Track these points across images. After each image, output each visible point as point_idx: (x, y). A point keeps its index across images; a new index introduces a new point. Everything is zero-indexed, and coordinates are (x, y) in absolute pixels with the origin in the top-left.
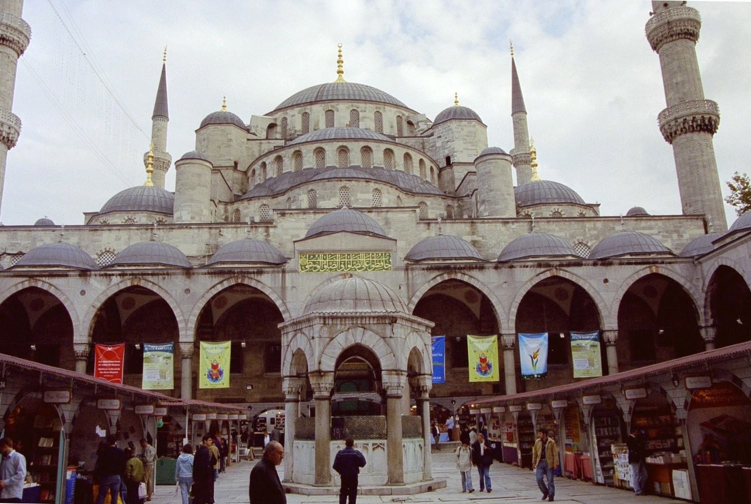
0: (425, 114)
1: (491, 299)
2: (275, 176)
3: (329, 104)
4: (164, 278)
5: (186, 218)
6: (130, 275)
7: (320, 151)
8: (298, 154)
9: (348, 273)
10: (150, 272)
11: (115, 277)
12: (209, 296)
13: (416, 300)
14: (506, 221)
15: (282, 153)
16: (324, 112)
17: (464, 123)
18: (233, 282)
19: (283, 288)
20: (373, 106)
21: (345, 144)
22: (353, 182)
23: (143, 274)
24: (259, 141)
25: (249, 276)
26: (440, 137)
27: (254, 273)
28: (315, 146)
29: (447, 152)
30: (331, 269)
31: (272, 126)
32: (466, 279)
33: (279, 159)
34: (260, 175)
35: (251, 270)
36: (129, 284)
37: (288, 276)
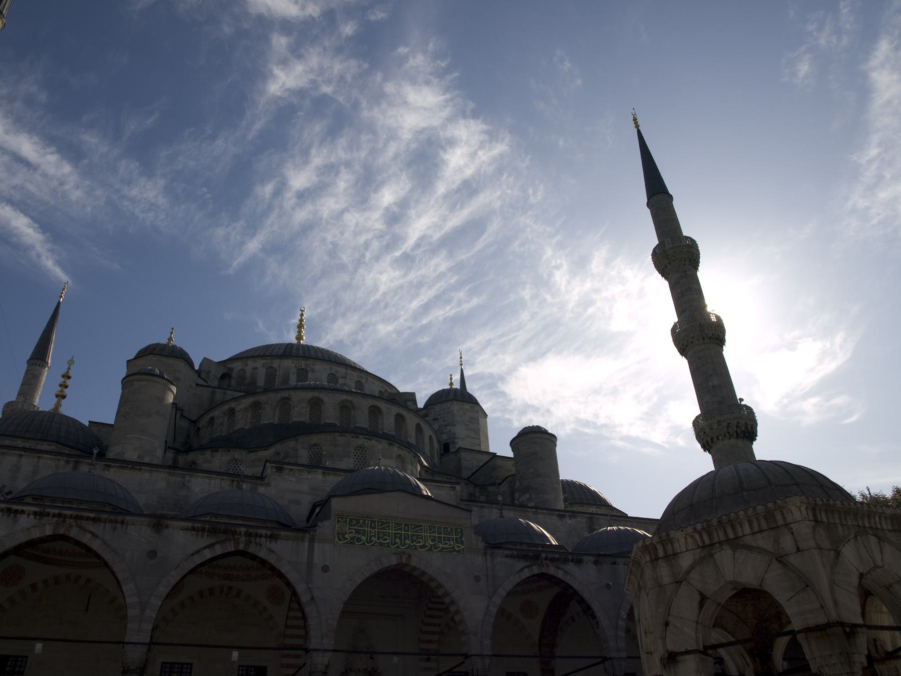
0: (413, 394)
1: (593, 606)
2: (247, 428)
3: (303, 362)
4: (115, 529)
5: (131, 455)
6: (54, 516)
7: (316, 404)
8: (286, 401)
9: (404, 552)
10: (92, 515)
11: (25, 516)
12: (190, 565)
13: (497, 600)
14: (561, 515)
15: (262, 398)
16: (295, 370)
17: (467, 406)
18: (231, 548)
19: (310, 565)
20: (356, 374)
21: (350, 398)
22: (373, 442)
23: (77, 518)
24: (210, 389)
25: (258, 540)
26: (437, 419)
27: (266, 536)
28: (310, 395)
29: (445, 437)
30: (381, 544)
31: (224, 376)
32: (560, 574)
33: (256, 406)
34: (222, 424)
35: (263, 532)
36: (49, 531)
37: (316, 545)
